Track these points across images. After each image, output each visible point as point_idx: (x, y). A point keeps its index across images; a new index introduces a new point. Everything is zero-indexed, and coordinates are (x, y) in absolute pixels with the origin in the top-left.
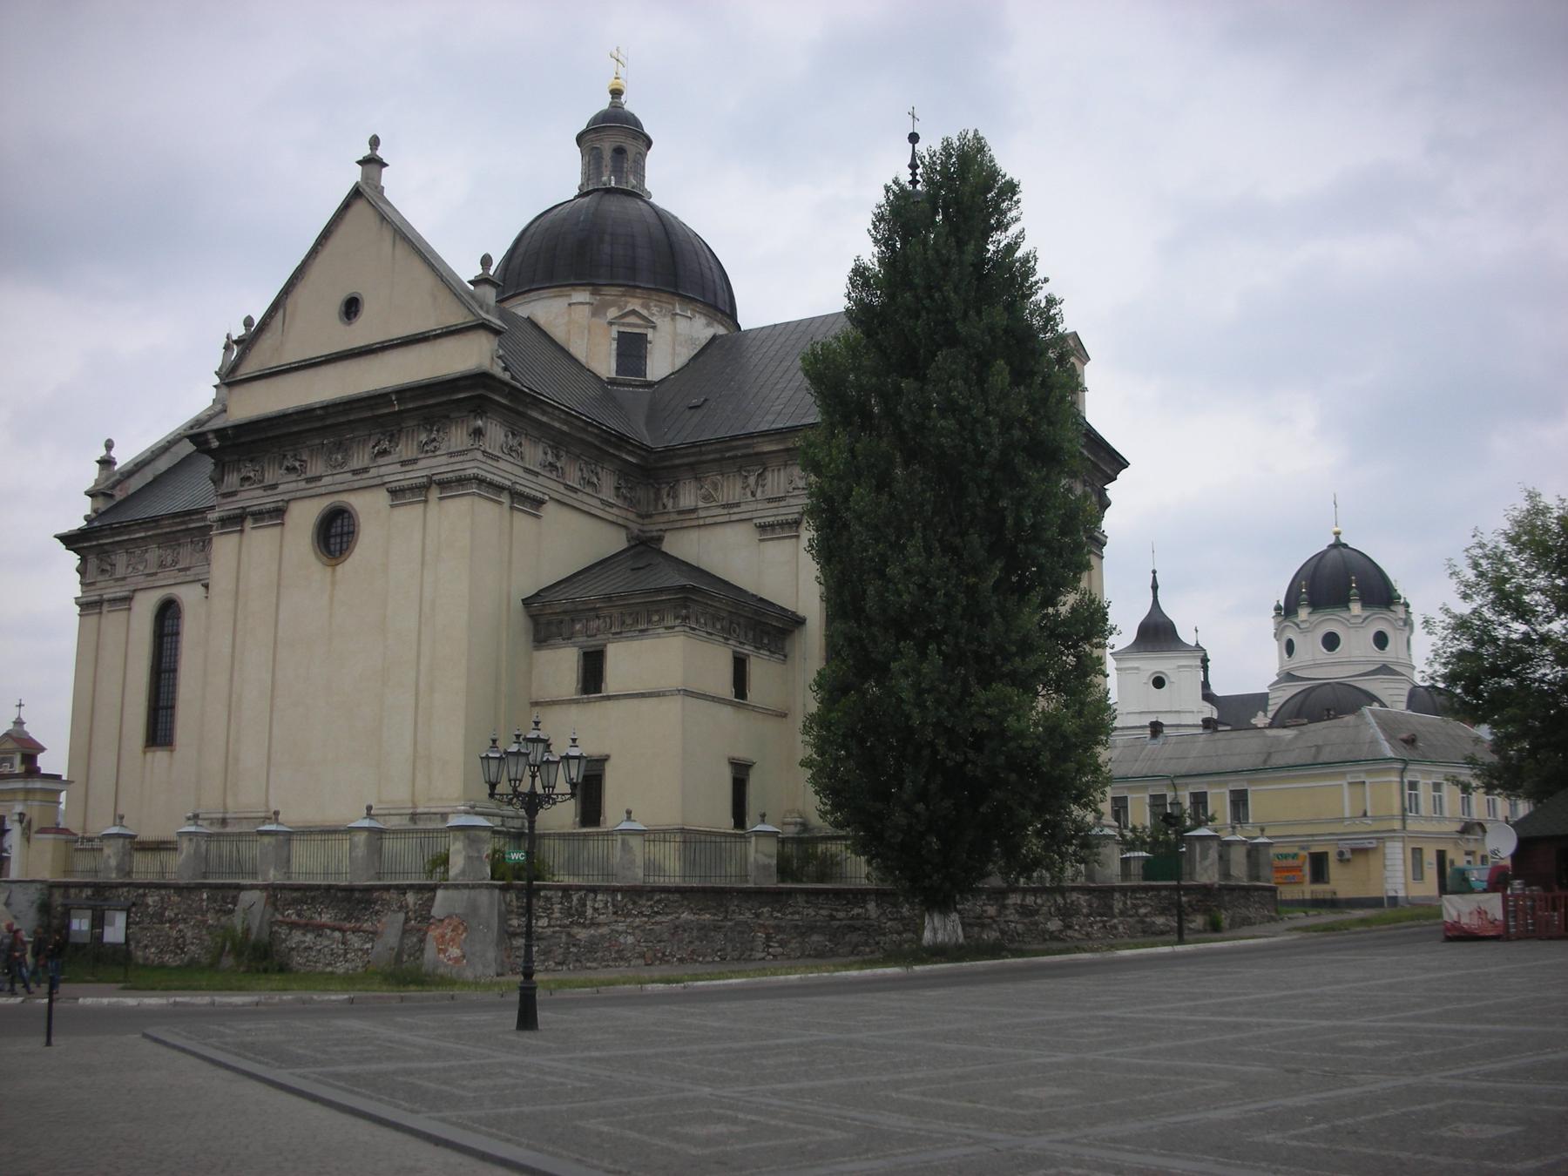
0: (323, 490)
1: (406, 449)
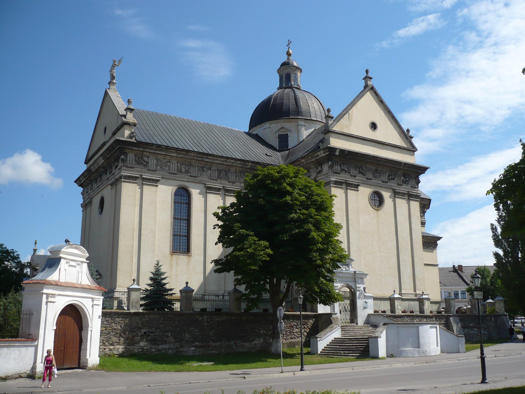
0: (373, 184)
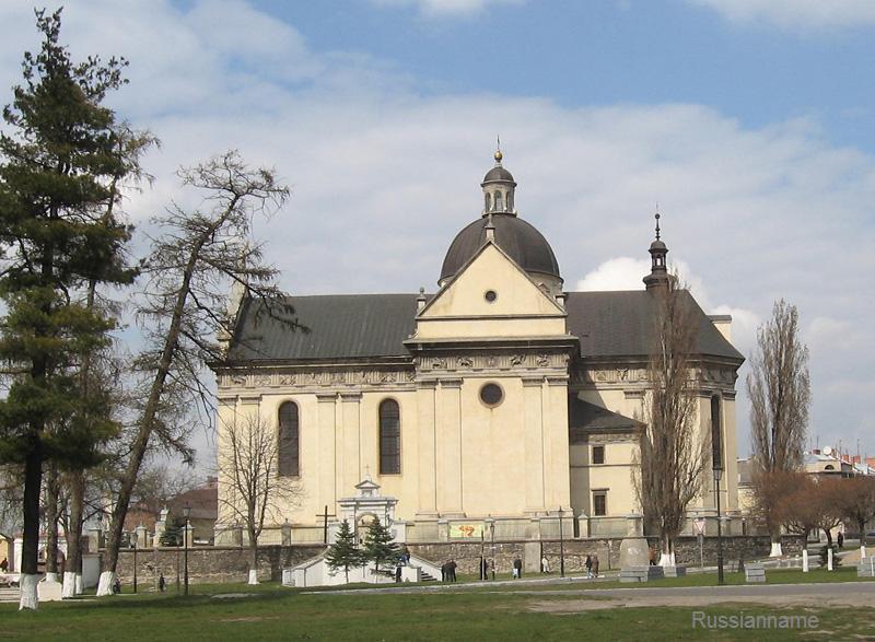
1: (529, 362)
